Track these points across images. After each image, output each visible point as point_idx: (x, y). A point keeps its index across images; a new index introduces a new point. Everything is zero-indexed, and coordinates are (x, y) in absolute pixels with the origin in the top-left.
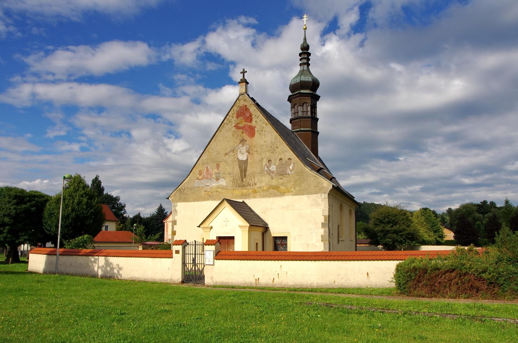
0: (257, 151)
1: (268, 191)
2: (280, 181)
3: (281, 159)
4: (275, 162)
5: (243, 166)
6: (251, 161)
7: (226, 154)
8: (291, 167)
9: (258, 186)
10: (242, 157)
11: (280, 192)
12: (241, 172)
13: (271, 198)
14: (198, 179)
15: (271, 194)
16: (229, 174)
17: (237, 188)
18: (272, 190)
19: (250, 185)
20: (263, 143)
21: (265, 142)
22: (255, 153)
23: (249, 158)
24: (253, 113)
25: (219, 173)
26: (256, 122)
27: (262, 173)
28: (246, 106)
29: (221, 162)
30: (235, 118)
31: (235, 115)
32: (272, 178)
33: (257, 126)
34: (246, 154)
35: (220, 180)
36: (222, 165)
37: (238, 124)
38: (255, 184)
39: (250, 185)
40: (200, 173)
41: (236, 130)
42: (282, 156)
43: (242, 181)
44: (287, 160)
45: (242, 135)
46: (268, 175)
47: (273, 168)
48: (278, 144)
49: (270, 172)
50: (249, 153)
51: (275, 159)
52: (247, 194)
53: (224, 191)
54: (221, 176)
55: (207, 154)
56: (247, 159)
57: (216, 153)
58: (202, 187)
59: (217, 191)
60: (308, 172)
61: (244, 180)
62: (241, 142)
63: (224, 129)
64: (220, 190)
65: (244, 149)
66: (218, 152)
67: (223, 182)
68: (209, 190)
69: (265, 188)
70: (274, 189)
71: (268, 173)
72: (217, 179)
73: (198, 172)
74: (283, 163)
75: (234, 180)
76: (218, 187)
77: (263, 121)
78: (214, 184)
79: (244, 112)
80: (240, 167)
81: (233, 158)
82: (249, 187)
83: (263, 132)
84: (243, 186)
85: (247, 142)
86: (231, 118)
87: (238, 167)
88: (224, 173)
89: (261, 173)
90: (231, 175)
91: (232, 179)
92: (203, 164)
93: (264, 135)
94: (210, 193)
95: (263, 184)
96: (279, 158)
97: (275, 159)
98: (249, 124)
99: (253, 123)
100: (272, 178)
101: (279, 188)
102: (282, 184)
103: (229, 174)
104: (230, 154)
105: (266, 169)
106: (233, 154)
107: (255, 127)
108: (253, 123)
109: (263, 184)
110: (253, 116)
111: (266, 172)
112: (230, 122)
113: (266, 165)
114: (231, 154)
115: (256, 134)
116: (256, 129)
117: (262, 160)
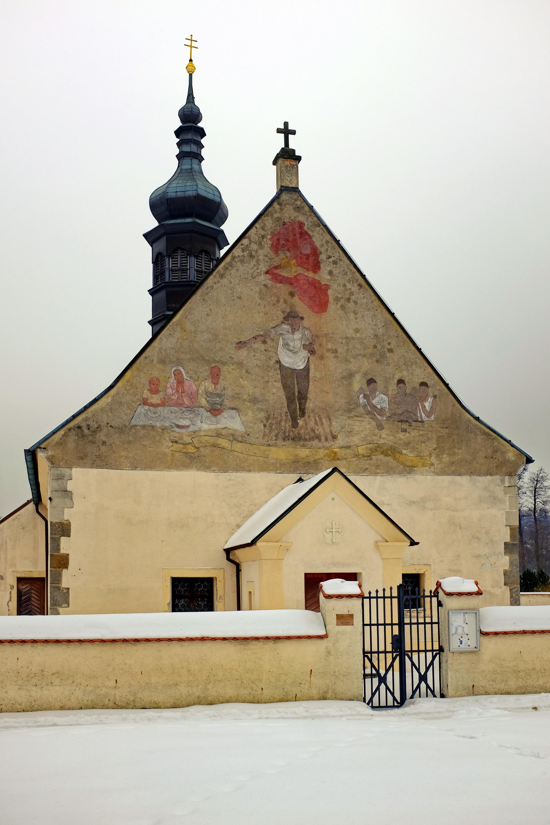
0: (335, 351)
1: (369, 457)
2: (401, 435)
3: (401, 381)
4: (386, 387)
5: (296, 388)
6: (318, 375)
7: (241, 345)
8: (427, 405)
9: (341, 441)
10: (296, 361)
11: (402, 464)
12: (290, 400)
13: (379, 478)
14: (145, 402)
15: (377, 467)
16: (254, 400)
17: (280, 442)
18: (381, 457)
19: (318, 437)
20: (350, 333)
21: (357, 331)
22: (330, 355)
23: (312, 367)
24: (323, 250)
25: (219, 395)
26: (330, 273)
27: (350, 408)
28: (301, 225)
29: (224, 364)
30: (267, 249)
31: (267, 243)
32: (380, 427)
33: (334, 286)
34: (304, 354)
35: (225, 414)
36: (229, 374)
37: (276, 268)
38: (334, 437)
39: (318, 437)
40: (154, 386)
41: (270, 283)
42: (404, 375)
43: (295, 424)
44: (418, 386)
45: (289, 299)
46: (367, 419)
47: (381, 400)
48: (393, 343)
49: (373, 411)
50: (312, 352)
51: (387, 381)
52: (311, 459)
53: (238, 446)
54: (227, 403)
55: (178, 334)
56: (307, 369)
57: (206, 336)
58: (164, 429)
59: (215, 445)
60: (469, 421)
61: (301, 422)
62: (286, 318)
63: (233, 272)
64: (224, 443)
65: (296, 339)
66: (216, 336)
67: (231, 422)
68: (187, 439)
69: (361, 450)
70: (387, 455)
71: (368, 413)
72: (215, 411)
73: (144, 380)
74: (408, 391)
75: (268, 419)
76: (219, 435)
77: (349, 276)
78: (206, 425)
79: (295, 241)
80: (285, 386)
81: (263, 358)
82: (315, 443)
83: (351, 305)
84: (297, 439)
85: (305, 323)
86: (254, 247)
87: (279, 385)
88: (236, 397)
89: (350, 411)
90: (259, 406)
91: (262, 415)
92: (162, 361)
93: (355, 313)
94: (191, 449)
95: (356, 440)
96: (397, 377)
97: (387, 381)
98: (310, 274)
99: (323, 276)
100: (380, 427)
101: (400, 453)
102: (407, 444)
103: (254, 400)
104: (256, 346)
105: (362, 400)
106: (263, 347)
107: (327, 287)
108: (323, 276)
109: (356, 440)
110: (323, 257)
111: (361, 410)
112: (251, 256)
113: (361, 390)
114: (258, 345)
115: (332, 306)
116: (330, 292)
117: (351, 376)
